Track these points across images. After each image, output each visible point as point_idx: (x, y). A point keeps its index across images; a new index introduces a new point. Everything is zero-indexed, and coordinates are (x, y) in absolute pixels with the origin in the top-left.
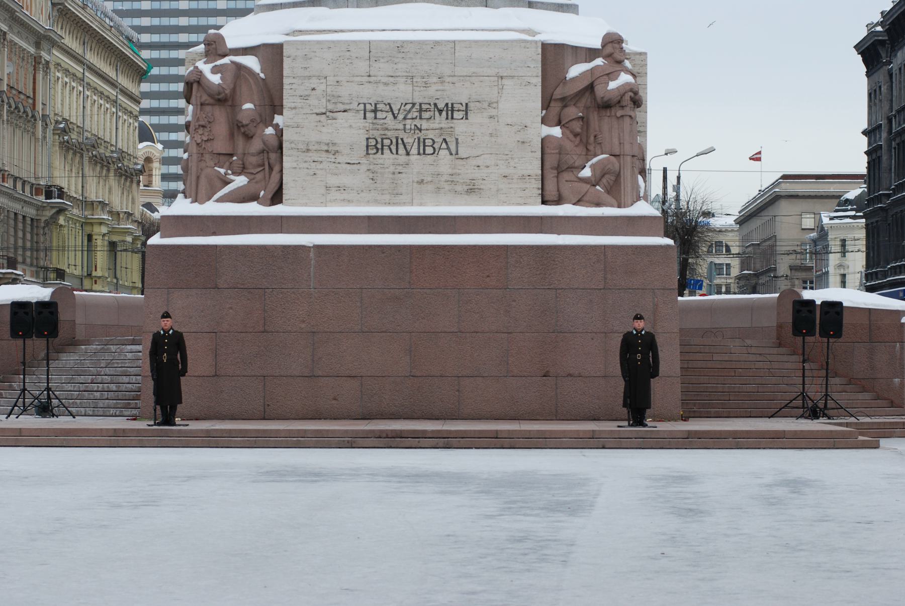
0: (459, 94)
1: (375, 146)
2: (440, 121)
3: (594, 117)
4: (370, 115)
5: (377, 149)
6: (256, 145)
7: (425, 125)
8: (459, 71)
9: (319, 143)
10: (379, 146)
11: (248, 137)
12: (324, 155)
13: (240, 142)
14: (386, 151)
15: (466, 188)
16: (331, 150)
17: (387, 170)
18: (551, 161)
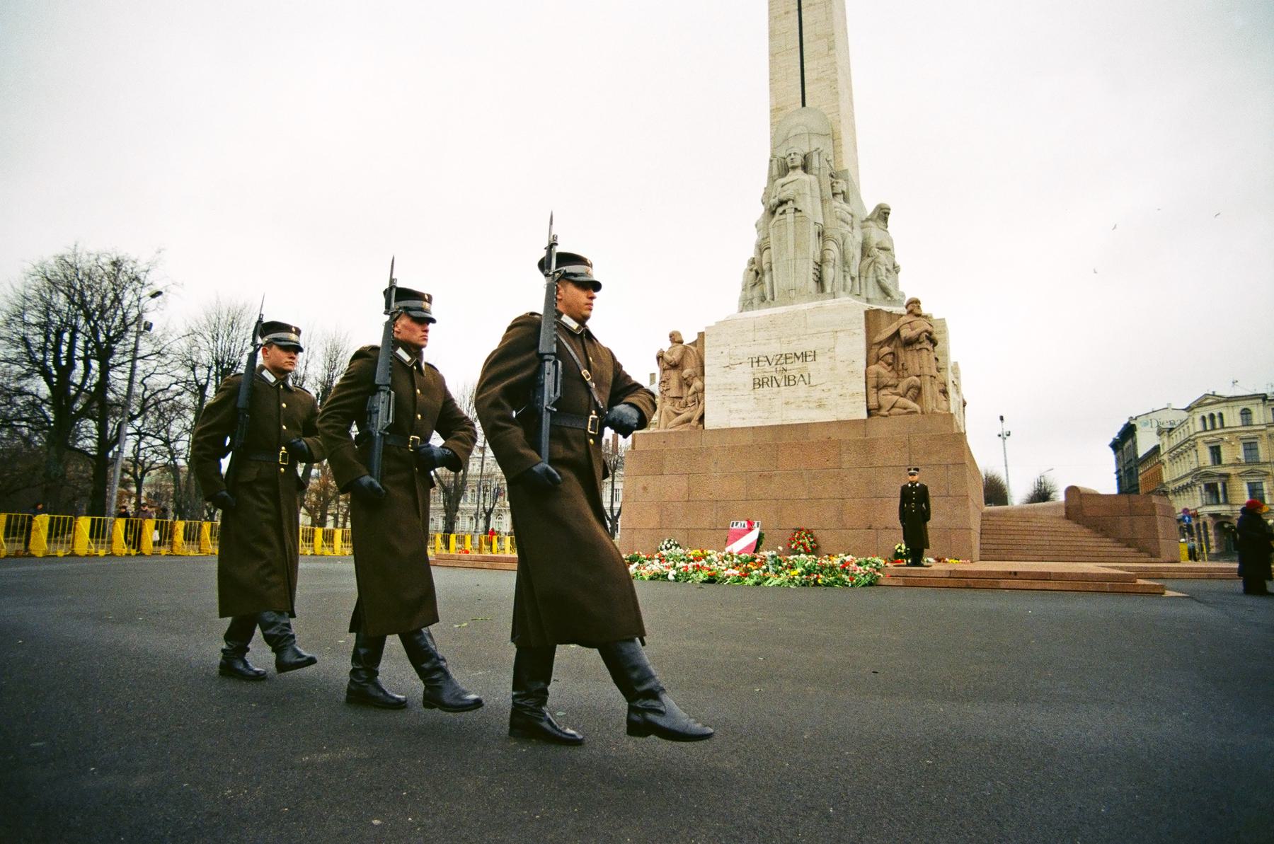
0: (808, 346)
1: (758, 383)
2: (798, 364)
3: (901, 353)
4: (755, 365)
6: (692, 389)
7: (788, 367)
8: (809, 331)
11: (689, 386)
13: (685, 388)
16: (731, 388)
18: (872, 382)
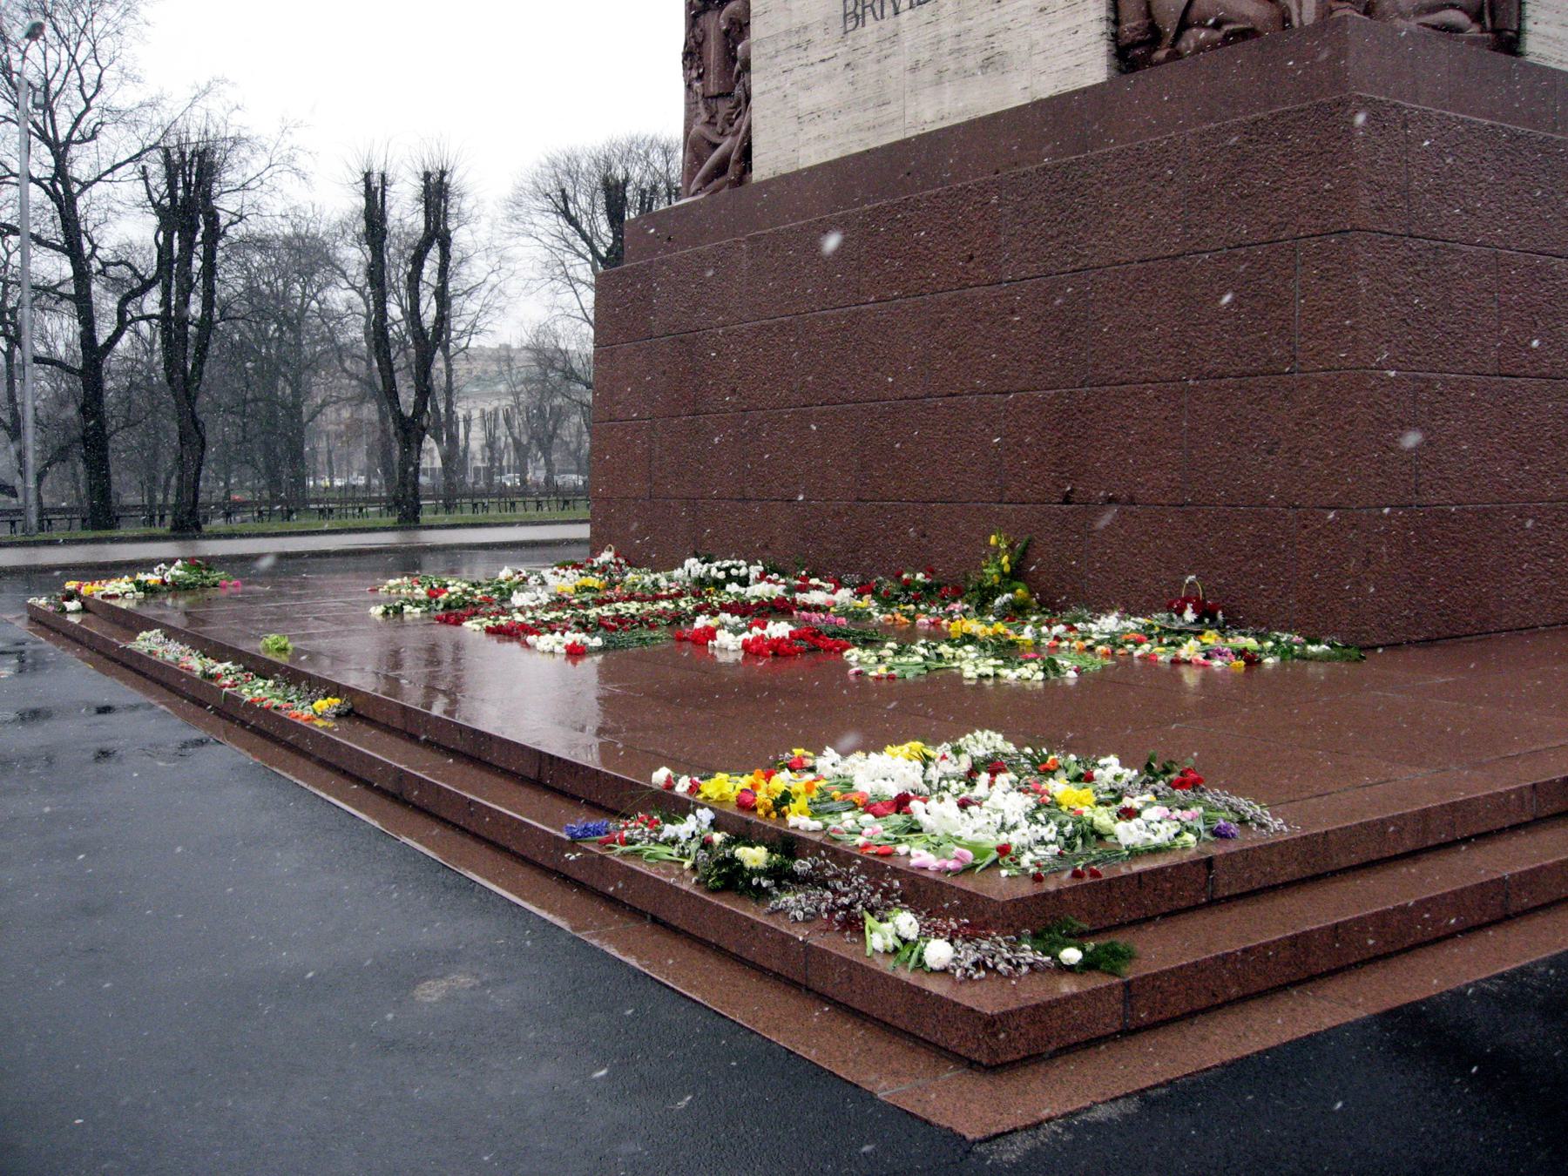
5: (857, 16)
9: (788, 33)
10: (859, 11)
12: (795, 54)
14: (869, 17)
15: (980, 58)
17: (872, 56)
